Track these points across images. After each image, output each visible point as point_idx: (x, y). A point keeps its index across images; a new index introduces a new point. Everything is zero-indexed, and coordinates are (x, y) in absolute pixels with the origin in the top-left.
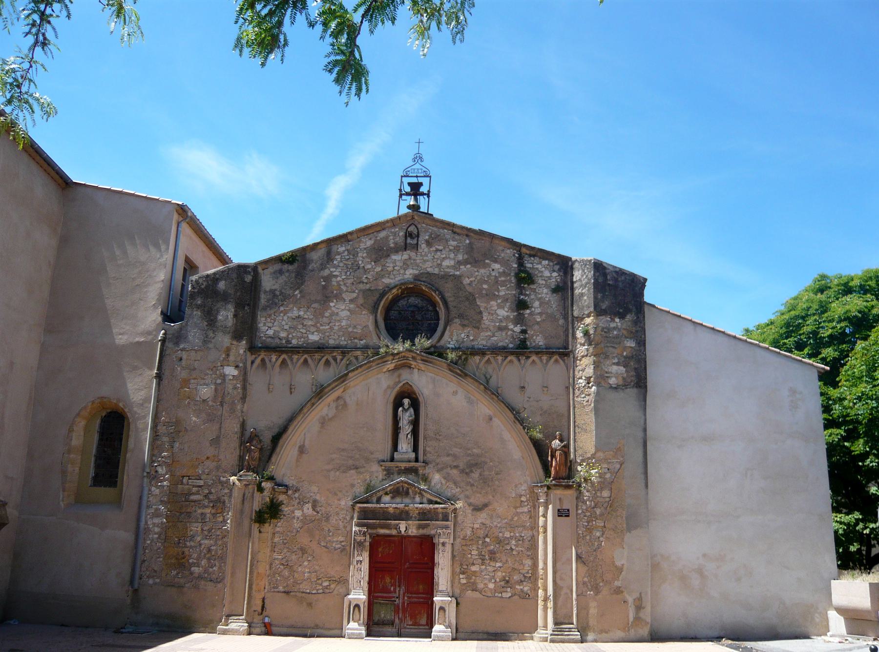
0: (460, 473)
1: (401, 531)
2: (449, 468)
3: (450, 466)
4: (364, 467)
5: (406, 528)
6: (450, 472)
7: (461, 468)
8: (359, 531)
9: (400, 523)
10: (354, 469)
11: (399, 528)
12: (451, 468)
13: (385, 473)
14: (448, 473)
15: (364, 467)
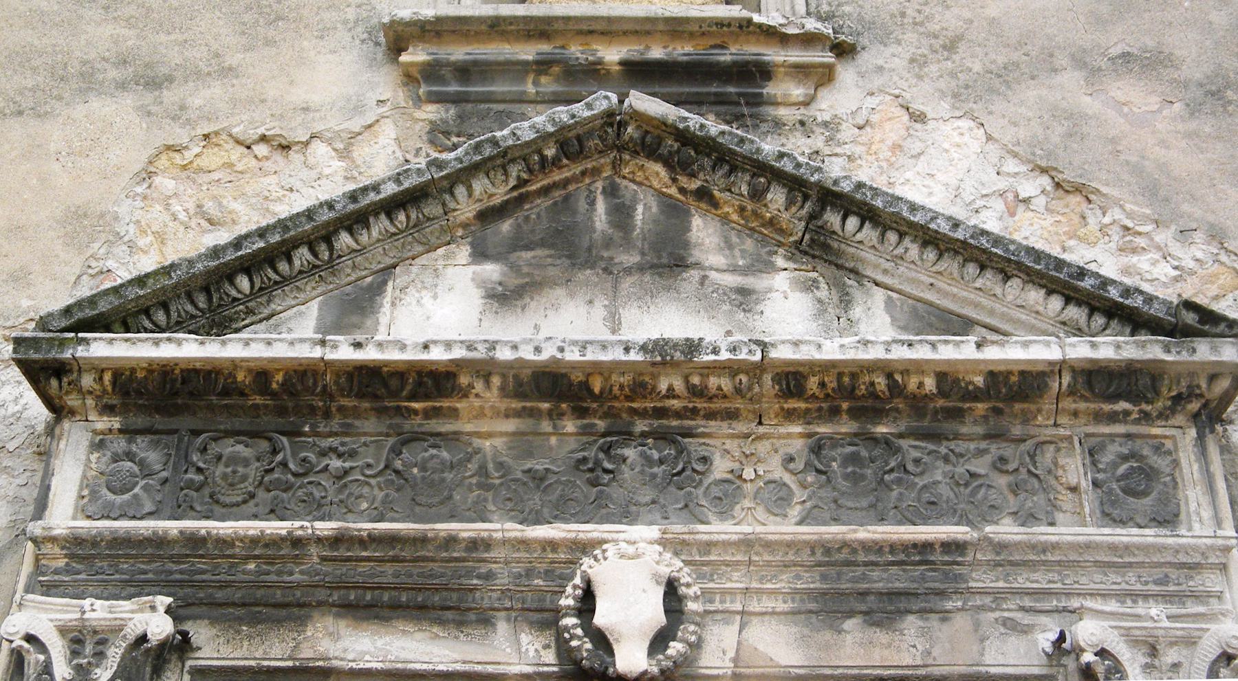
0: (1193, 110)
1: (602, 641)
2: (1071, 79)
3: (1080, 61)
4: (227, 72)
5: (672, 591)
6: (1090, 104)
7: (1194, 71)
8: (76, 638)
9: (585, 548)
10: (122, 86)
11: (588, 598)
12: (1093, 74)
13: (431, 112)
14: (1075, 123)
15: (227, 72)
